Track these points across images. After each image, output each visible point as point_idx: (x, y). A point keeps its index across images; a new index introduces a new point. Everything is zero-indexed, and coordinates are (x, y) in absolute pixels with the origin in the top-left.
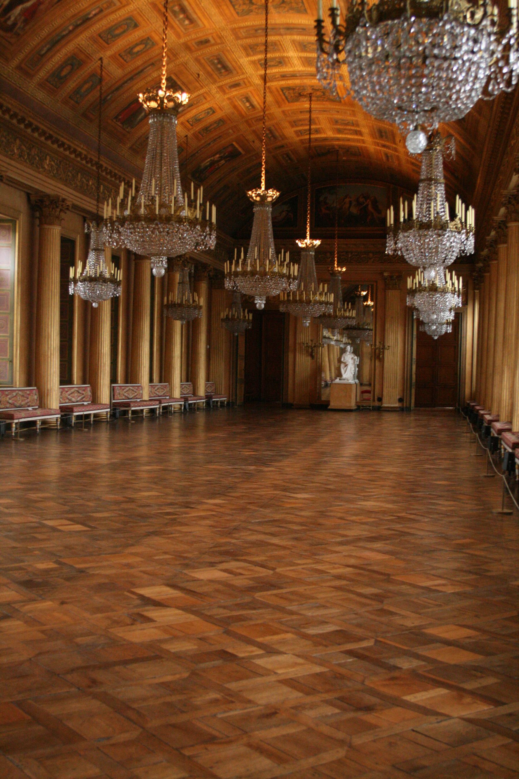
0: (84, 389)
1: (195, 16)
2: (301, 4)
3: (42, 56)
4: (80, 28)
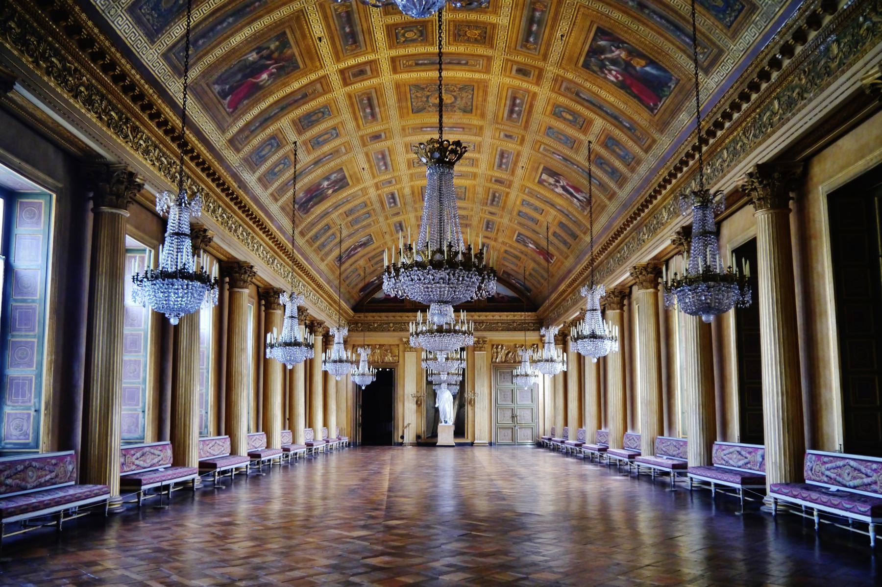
0: (751, 450)
1: (508, 102)
2: (413, 96)
3: (600, 184)
4: (572, 161)
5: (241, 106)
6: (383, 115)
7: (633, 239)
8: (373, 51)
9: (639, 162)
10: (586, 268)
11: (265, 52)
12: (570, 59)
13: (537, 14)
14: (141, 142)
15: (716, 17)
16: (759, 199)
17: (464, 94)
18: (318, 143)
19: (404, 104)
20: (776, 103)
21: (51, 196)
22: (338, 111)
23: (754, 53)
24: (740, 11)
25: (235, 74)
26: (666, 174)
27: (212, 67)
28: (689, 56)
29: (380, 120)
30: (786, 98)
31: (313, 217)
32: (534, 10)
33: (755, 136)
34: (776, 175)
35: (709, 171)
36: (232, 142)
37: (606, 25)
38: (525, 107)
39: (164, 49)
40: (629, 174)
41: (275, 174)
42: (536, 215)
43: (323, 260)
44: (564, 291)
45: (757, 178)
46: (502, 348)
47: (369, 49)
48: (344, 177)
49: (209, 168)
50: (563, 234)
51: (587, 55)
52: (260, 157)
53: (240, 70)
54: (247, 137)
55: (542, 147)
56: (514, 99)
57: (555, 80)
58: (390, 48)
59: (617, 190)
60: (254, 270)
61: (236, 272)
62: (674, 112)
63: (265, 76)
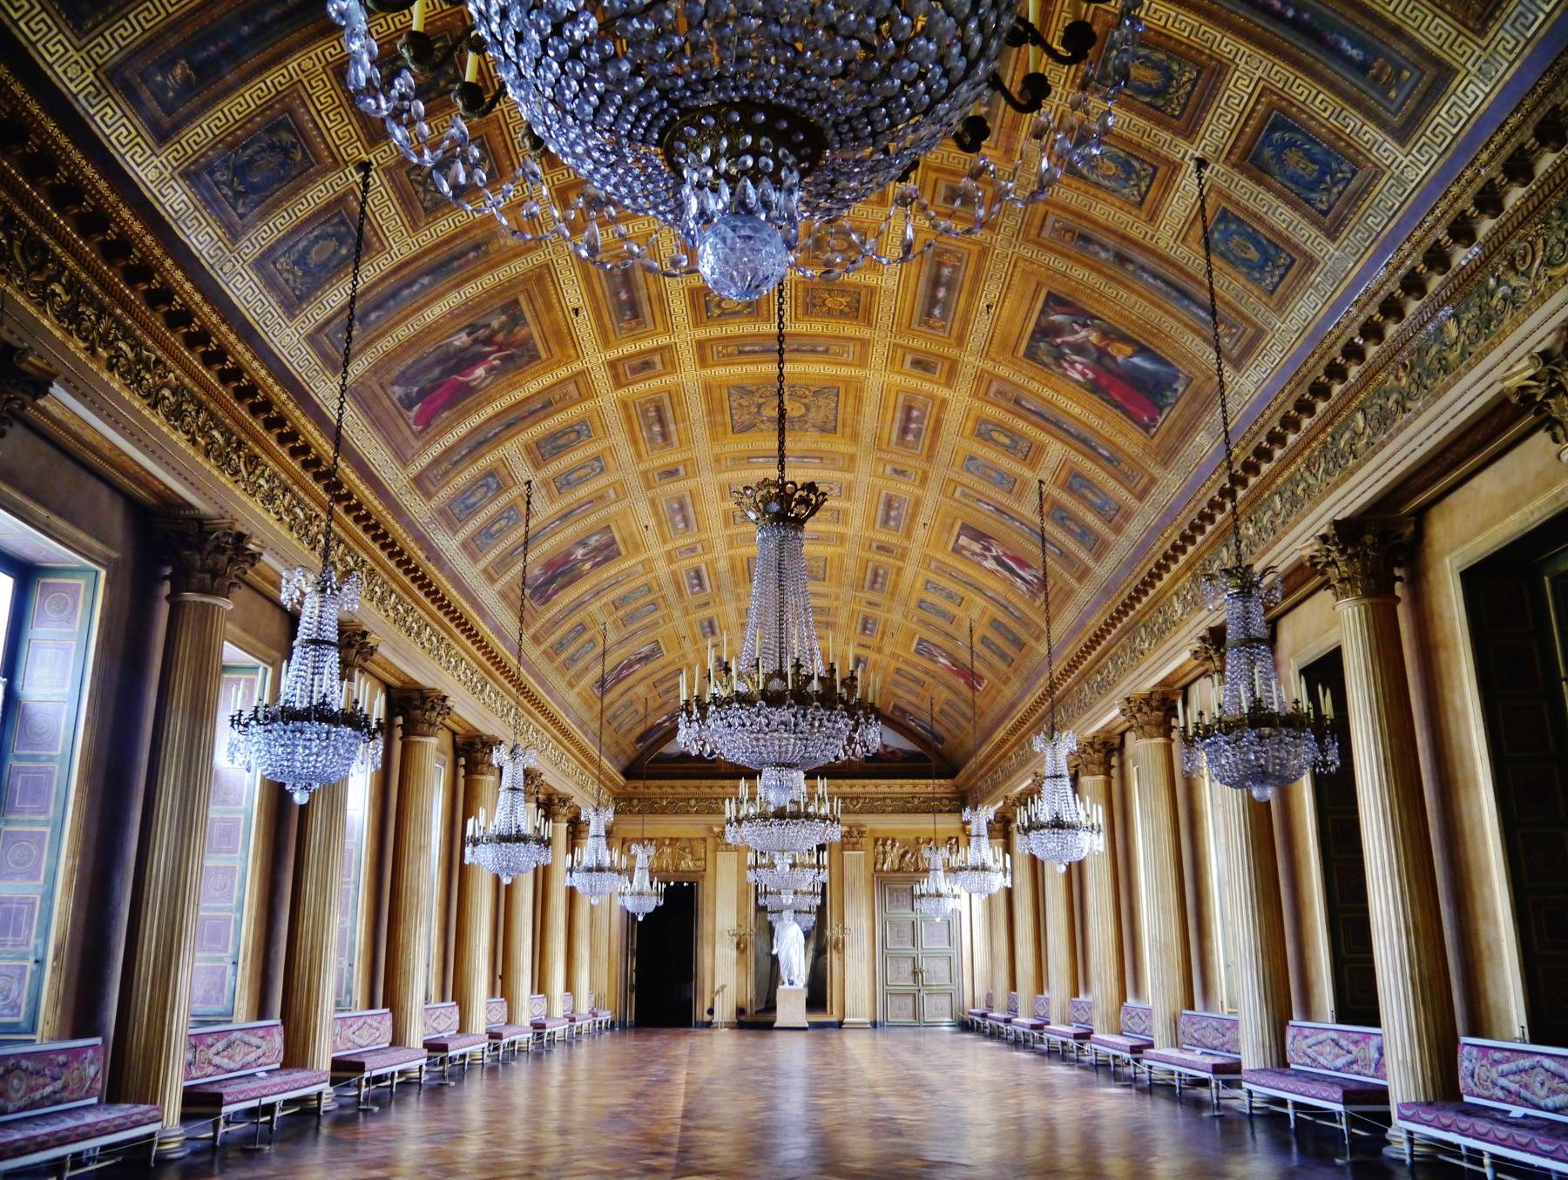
1: (898, 415)
2: (734, 405)
5: (435, 422)
6: (683, 436)
7: (1124, 648)
8: (666, 330)
9: (1128, 516)
10: (1040, 701)
11: (482, 333)
12: (1003, 345)
13: (946, 271)
14: (262, 482)
15: (1248, 276)
16: (1341, 581)
17: (822, 402)
18: (569, 483)
19: (719, 418)
20: (1359, 416)
21: (97, 573)
22: (605, 428)
23: (1316, 336)
24: (1288, 268)
25: (429, 368)
26: (1176, 536)
27: (390, 357)
28: (1205, 340)
29: (676, 444)
30: (1376, 408)
31: (556, 609)
32: (940, 265)
33: (1327, 472)
34: (1369, 539)
35: (1251, 532)
36: (418, 481)
37: (1061, 289)
38: (928, 423)
39: (310, 327)
40: (1112, 537)
41: (492, 536)
42: (951, 608)
43: (571, 686)
44: (1004, 741)
45: (1336, 544)
46: (893, 845)
47: (660, 328)
48: (613, 542)
49: (376, 526)
50: (999, 641)
51: (1032, 338)
52: (467, 508)
53: (439, 362)
54: (446, 473)
55: (959, 489)
56: (909, 409)
57: (979, 377)
58: (696, 325)
59: (1090, 562)
60: (449, 703)
61: (416, 708)
62: (1186, 431)
63: (480, 372)
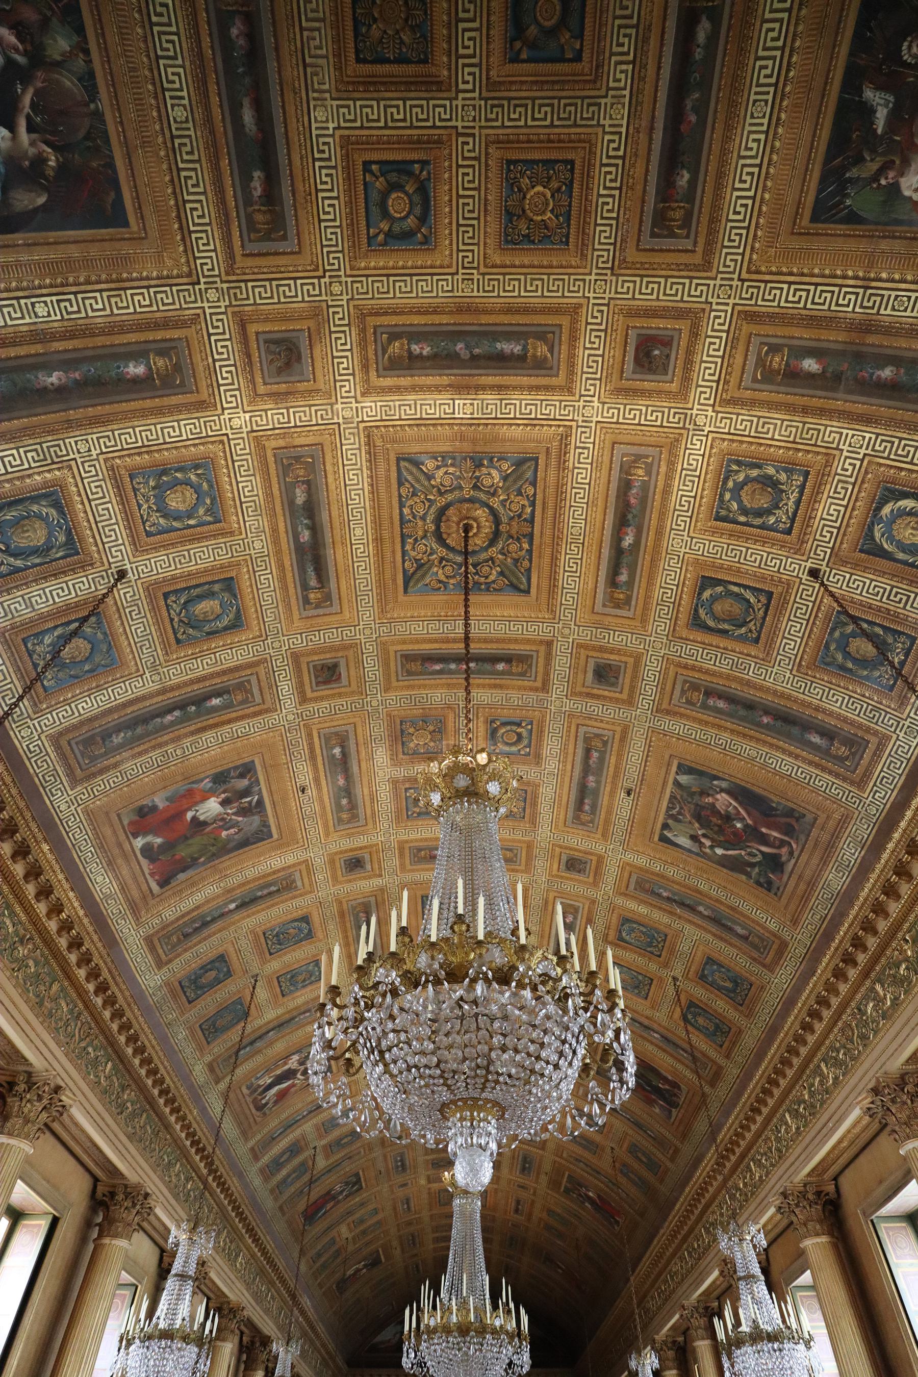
63: (591, 1194)
